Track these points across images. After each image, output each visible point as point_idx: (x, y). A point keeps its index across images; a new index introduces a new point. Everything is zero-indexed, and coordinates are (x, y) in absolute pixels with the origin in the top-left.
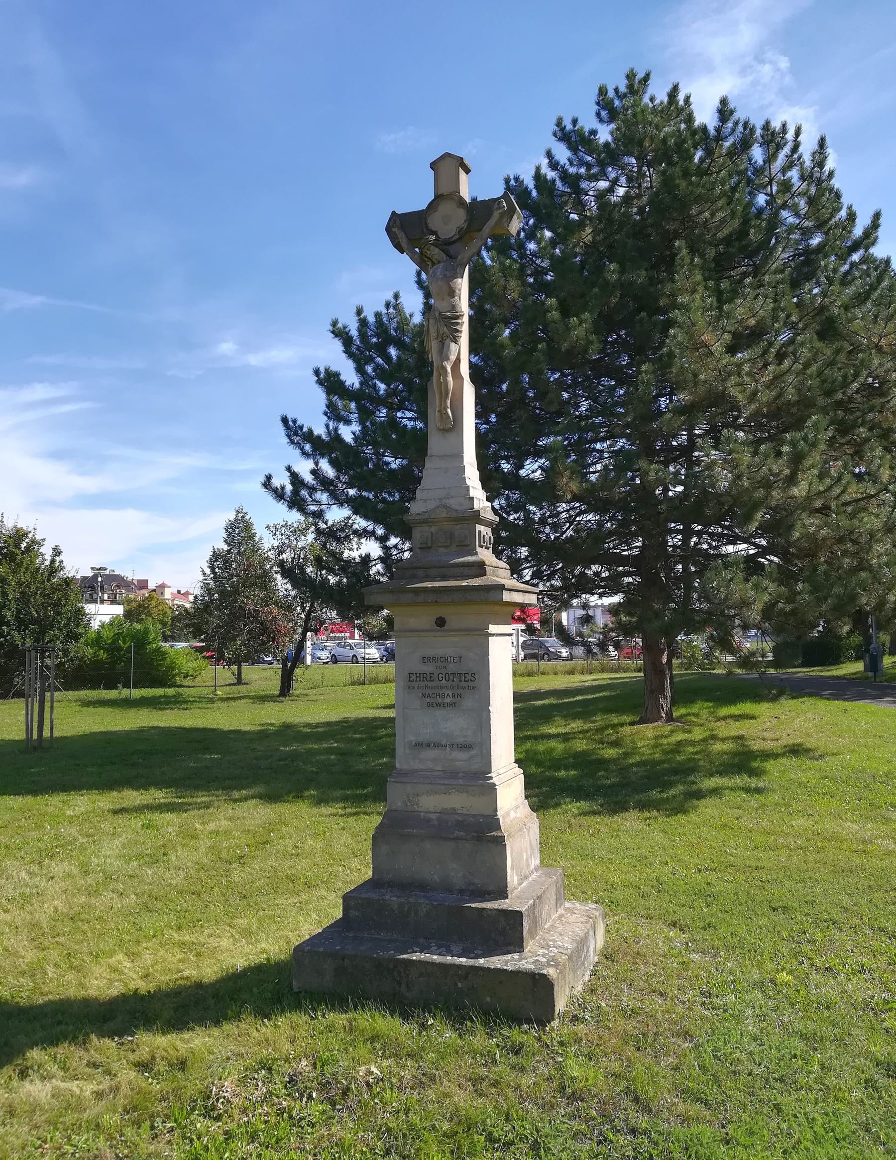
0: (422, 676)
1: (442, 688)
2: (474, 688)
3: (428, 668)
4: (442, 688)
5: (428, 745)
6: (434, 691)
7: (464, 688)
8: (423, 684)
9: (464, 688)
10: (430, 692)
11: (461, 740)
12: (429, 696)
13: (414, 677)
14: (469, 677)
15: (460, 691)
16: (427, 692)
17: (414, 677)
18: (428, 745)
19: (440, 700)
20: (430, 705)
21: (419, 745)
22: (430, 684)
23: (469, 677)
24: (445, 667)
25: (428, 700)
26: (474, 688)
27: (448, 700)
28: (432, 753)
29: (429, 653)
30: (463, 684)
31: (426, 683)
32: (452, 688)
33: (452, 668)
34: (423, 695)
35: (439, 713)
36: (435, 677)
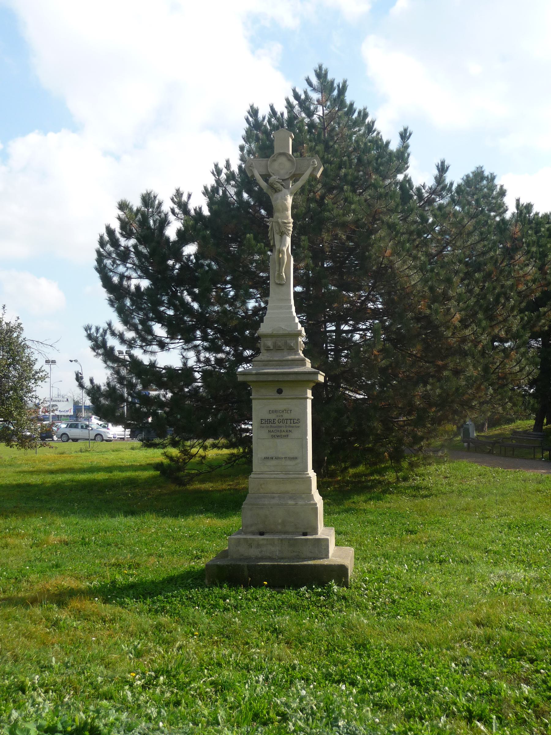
0: (268, 421)
1: (281, 427)
2: (298, 427)
3: (272, 416)
4: (281, 427)
5: (272, 458)
6: (275, 429)
7: (293, 427)
8: (269, 425)
9: (293, 427)
10: (274, 429)
11: (291, 455)
12: (273, 431)
13: (264, 421)
14: (295, 421)
15: (290, 429)
16: (271, 429)
17: (264, 421)
18: (272, 458)
19: (279, 434)
20: (273, 437)
21: (266, 458)
22: (273, 425)
23: (295, 421)
24: (282, 416)
25: (272, 434)
26: (298, 427)
27: (284, 434)
28: (274, 462)
29: (273, 408)
30: (292, 425)
31: (271, 424)
32: (286, 427)
33: (286, 416)
34: (269, 431)
35: (278, 441)
36: (276, 421)
